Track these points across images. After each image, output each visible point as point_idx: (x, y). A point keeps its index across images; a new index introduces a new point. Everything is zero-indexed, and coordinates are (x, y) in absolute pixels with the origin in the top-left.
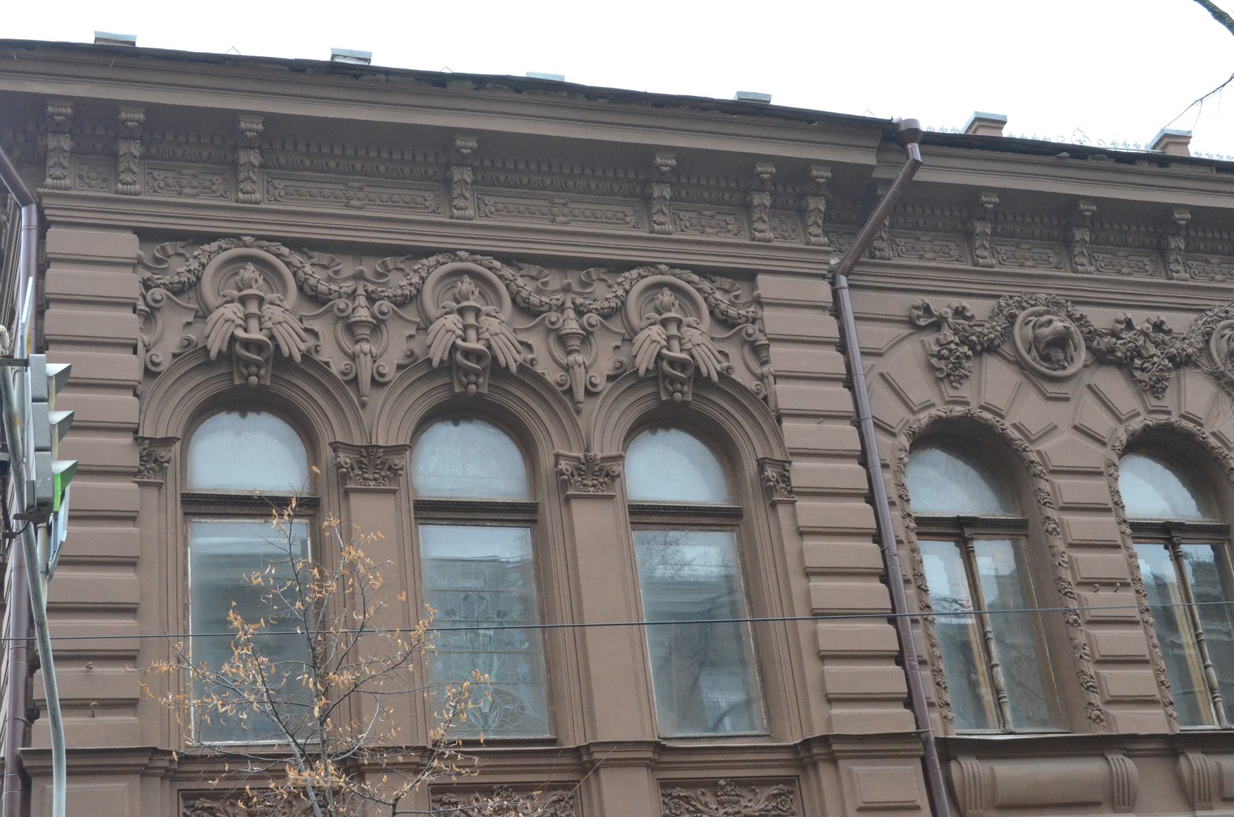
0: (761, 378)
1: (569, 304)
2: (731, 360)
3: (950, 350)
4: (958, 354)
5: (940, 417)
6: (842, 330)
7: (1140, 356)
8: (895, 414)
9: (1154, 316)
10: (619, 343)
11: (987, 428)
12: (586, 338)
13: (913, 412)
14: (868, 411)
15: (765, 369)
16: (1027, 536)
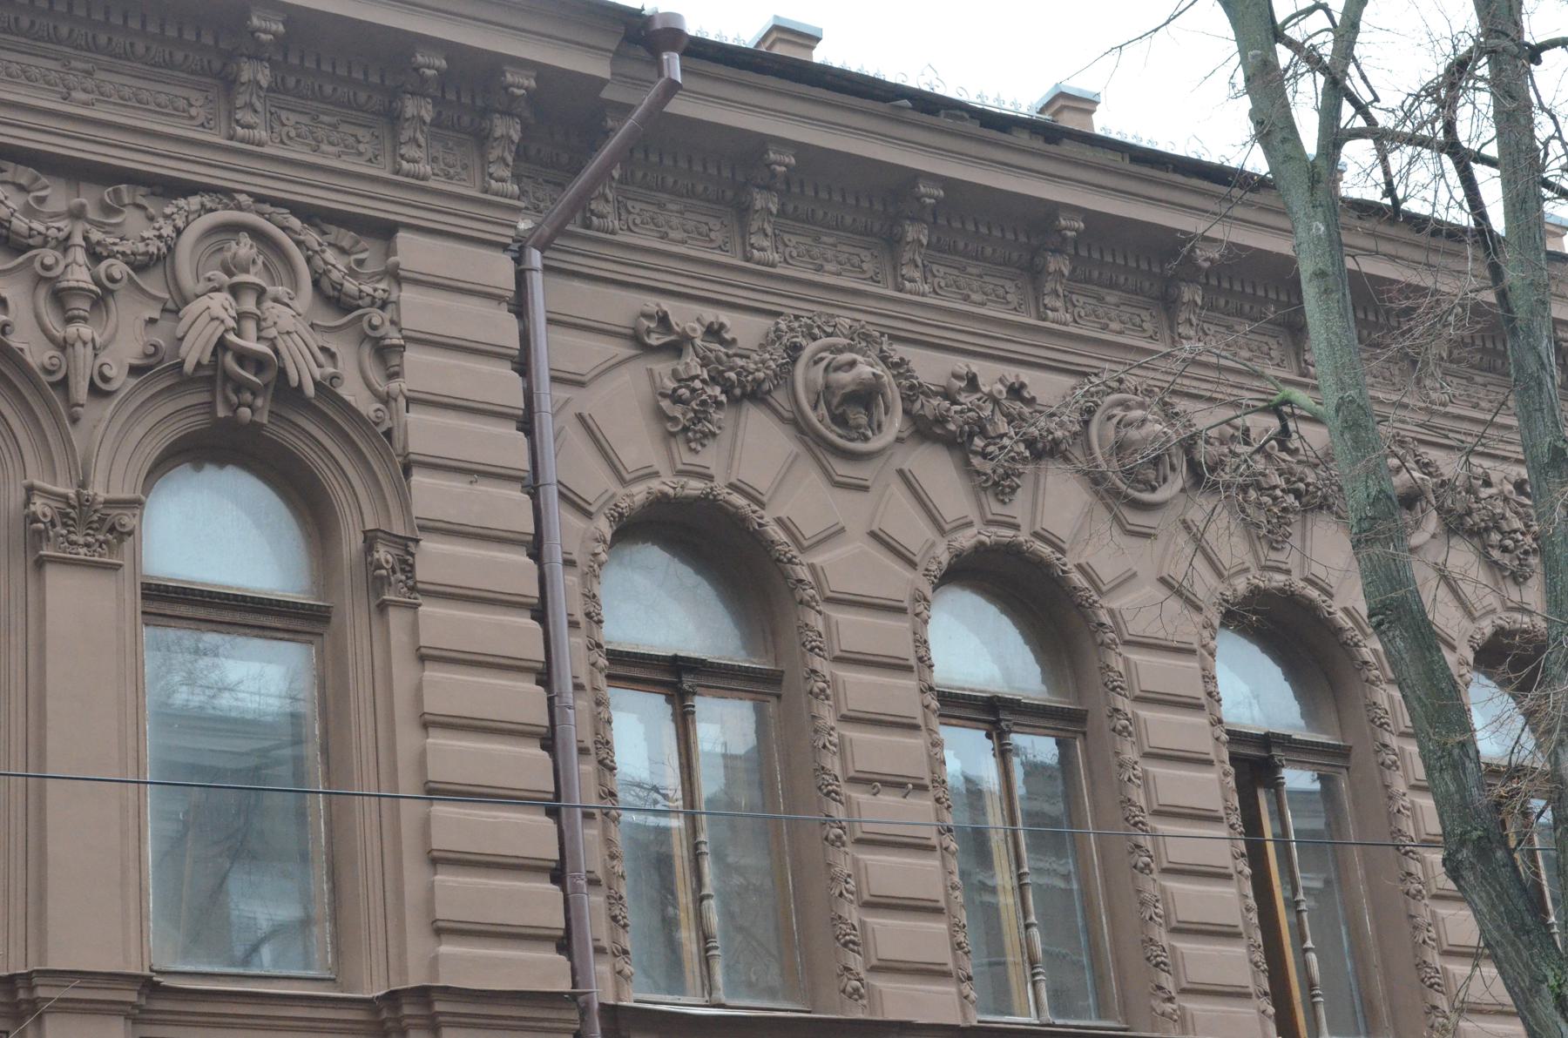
0: (386, 400)
1: (78, 239)
2: (340, 363)
3: (693, 390)
4: (704, 397)
5: (665, 495)
6: (525, 337)
7: (983, 433)
8: (594, 482)
9: (1013, 373)
10: (156, 315)
11: (737, 521)
12: (101, 299)
13: (623, 482)
14: (551, 472)
15: (394, 386)
16: (779, 697)
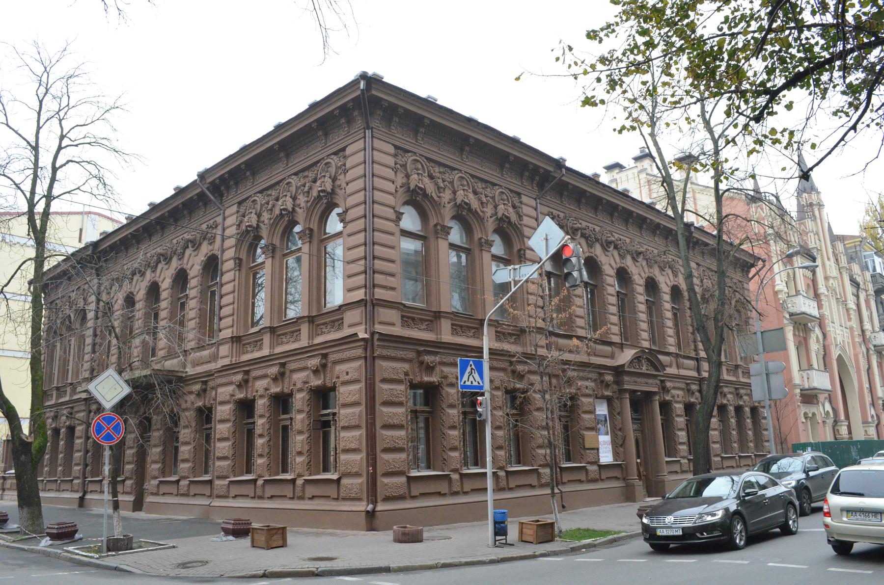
6: (537, 215)
15: (522, 222)
